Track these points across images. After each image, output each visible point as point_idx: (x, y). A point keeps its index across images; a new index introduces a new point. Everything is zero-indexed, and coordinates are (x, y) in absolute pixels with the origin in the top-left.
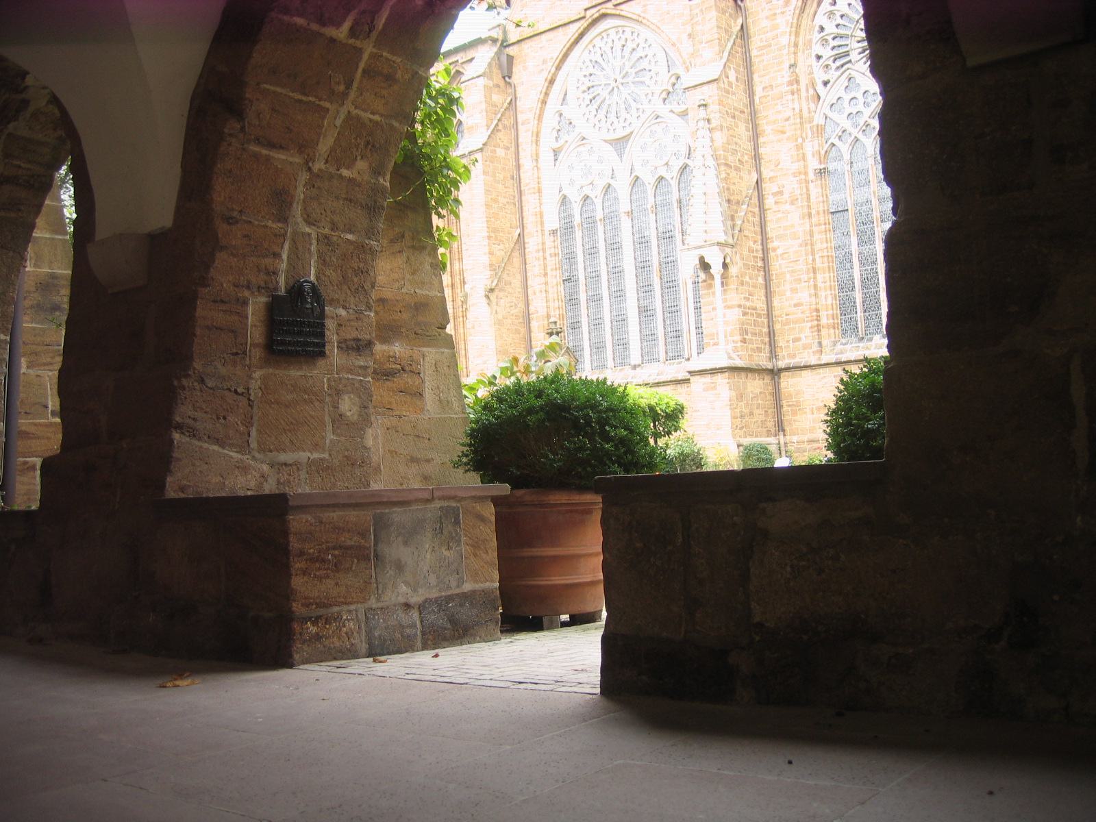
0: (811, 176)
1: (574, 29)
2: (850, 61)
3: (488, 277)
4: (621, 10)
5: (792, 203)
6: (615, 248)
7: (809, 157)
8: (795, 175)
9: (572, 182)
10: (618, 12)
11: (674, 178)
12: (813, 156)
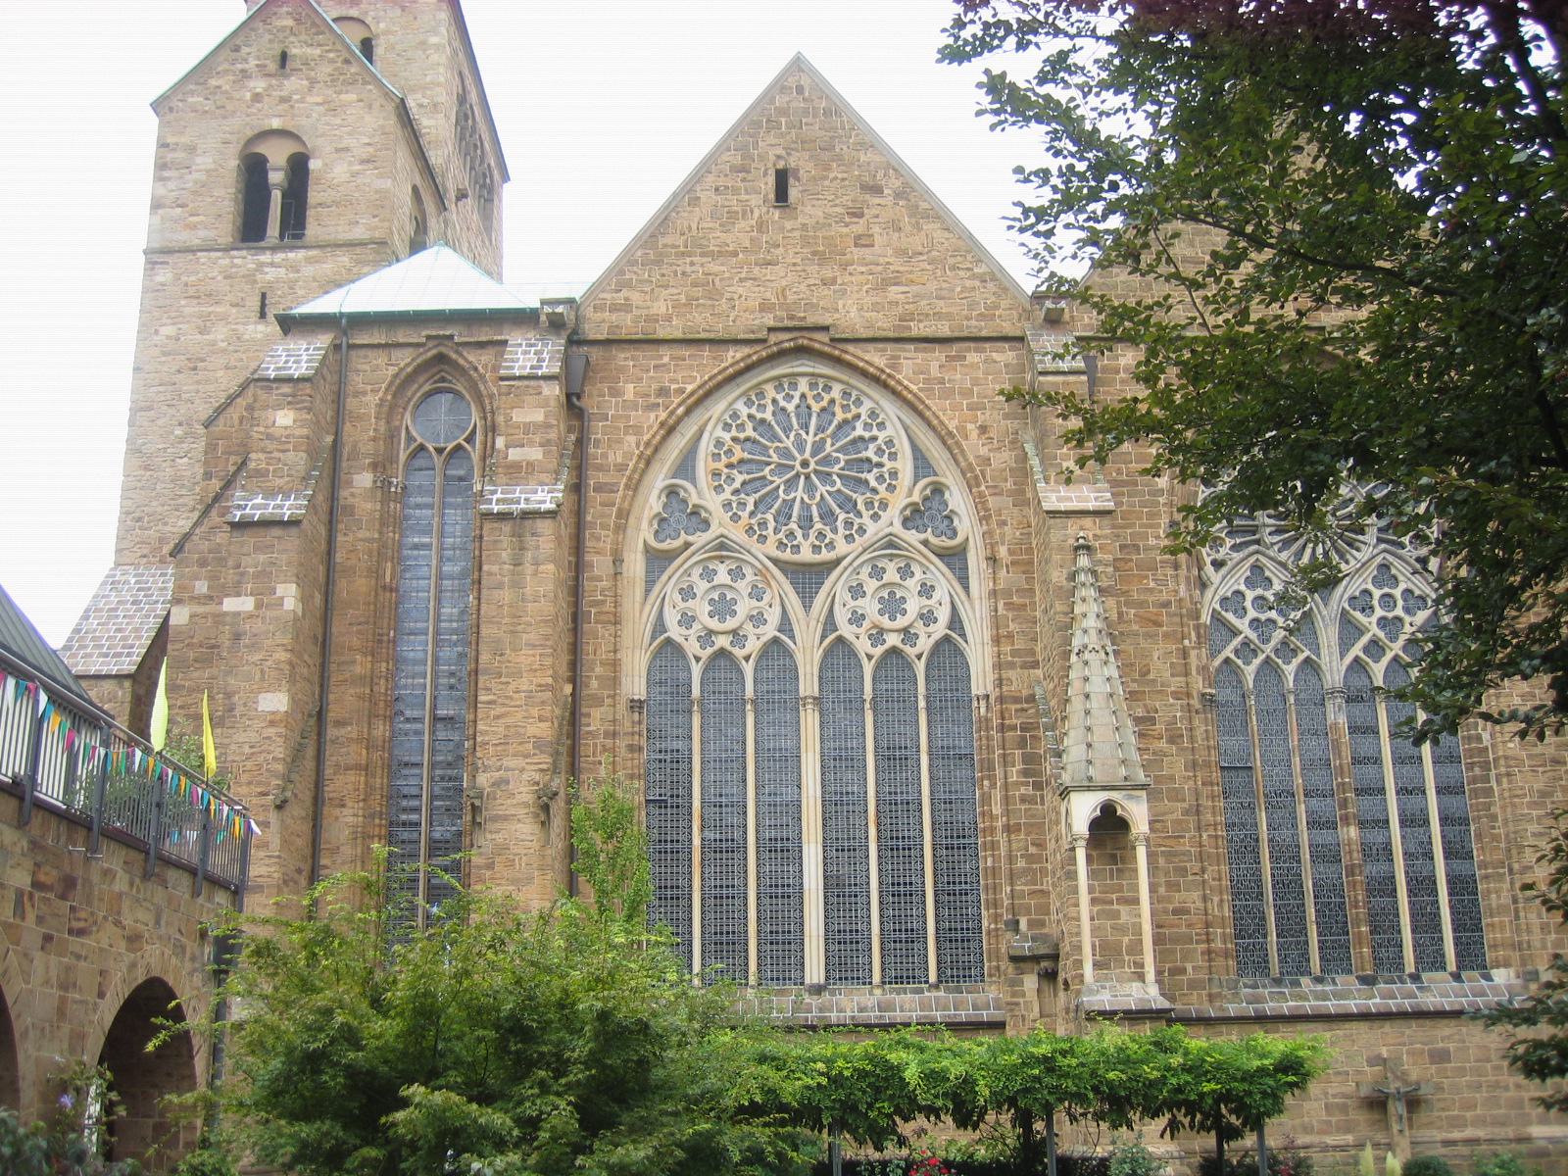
0: (1196, 703)
1: (734, 355)
2: (1257, 542)
3: (545, 766)
4: (846, 352)
5: (1172, 740)
6: (782, 762)
7: (1194, 673)
8: (1176, 695)
9: (687, 620)
10: (837, 352)
12: (1198, 673)
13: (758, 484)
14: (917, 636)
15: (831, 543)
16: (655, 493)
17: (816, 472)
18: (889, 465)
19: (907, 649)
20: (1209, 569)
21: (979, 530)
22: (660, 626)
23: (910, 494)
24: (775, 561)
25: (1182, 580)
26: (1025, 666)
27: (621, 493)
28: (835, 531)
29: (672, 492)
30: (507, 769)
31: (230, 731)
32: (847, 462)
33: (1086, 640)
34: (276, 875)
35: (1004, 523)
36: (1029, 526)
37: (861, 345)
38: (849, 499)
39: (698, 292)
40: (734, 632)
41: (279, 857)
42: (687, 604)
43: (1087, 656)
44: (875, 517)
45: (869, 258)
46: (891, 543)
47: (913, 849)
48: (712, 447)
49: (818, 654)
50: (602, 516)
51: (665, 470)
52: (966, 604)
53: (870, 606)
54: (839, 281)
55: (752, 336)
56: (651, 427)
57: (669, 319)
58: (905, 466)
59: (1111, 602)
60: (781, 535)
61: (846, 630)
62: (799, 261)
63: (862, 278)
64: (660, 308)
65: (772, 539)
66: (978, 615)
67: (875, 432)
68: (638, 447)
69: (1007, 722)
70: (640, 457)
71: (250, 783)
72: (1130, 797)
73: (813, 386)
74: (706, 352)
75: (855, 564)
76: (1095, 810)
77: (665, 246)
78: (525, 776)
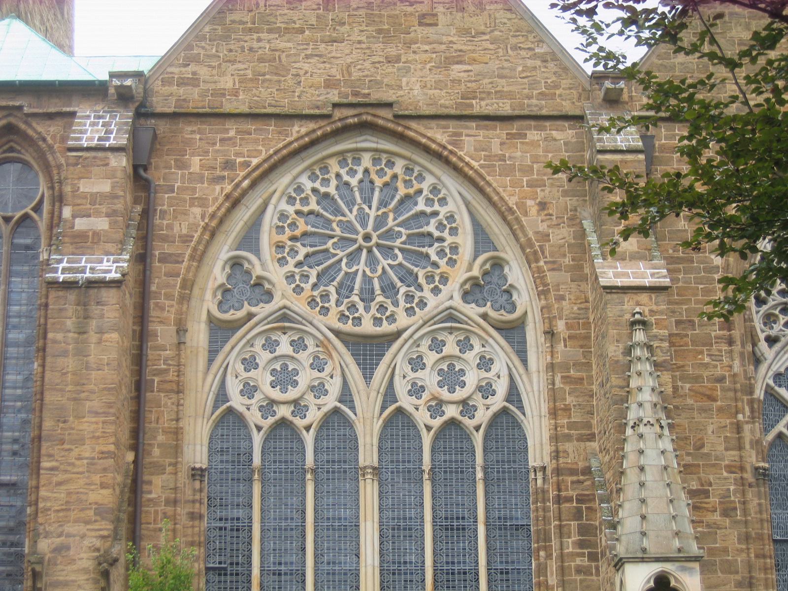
0: (749, 476)
1: (299, 130)
3: (105, 533)
4: (409, 128)
5: (725, 513)
7: (748, 446)
8: (730, 469)
9: (249, 390)
10: (400, 129)
11: (482, 431)
12: (752, 447)
13: (320, 257)
14: (475, 408)
15: (392, 315)
16: (219, 264)
17: (378, 245)
18: (449, 240)
19: (466, 421)
20: (763, 345)
21: (537, 304)
22: (222, 396)
23: (470, 268)
24: (337, 333)
25: (736, 356)
26: (580, 439)
27: (185, 264)
28: (396, 304)
29: (236, 263)
30: (69, 535)
32: (409, 236)
33: (641, 414)
35: (562, 298)
36: (587, 302)
37: (426, 122)
38: (410, 272)
39: (264, 67)
40: (295, 402)
42: (250, 374)
43: (642, 429)
44: (436, 291)
45: (434, 37)
46: (450, 316)
47: (414, 532)
48: (276, 221)
49: (378, 425)
50: (168, 286)
51: (230, 241)
52: (524, 377)
53: (429, 378)
54: (403, 60)
55: (317, 112)
56: (216, 199)
57: (235, 93)
58: (466, 241)
59: (666, 377)
60: (342, 308)
61: (406, 401)
62: (364, 39)
63: (425, 56)
64: (227, 82)
65: (334, 311)
66: (535, 388)
67: (436, 207)
68: (203, 217)
69: (563, 494)
70: (205, 228)
72: (684, 569)
73: (376, 161)
74: (272, 127)
75: (416, 336)
76: (648, 581)
77: (233, 22)
78: (86, 543)
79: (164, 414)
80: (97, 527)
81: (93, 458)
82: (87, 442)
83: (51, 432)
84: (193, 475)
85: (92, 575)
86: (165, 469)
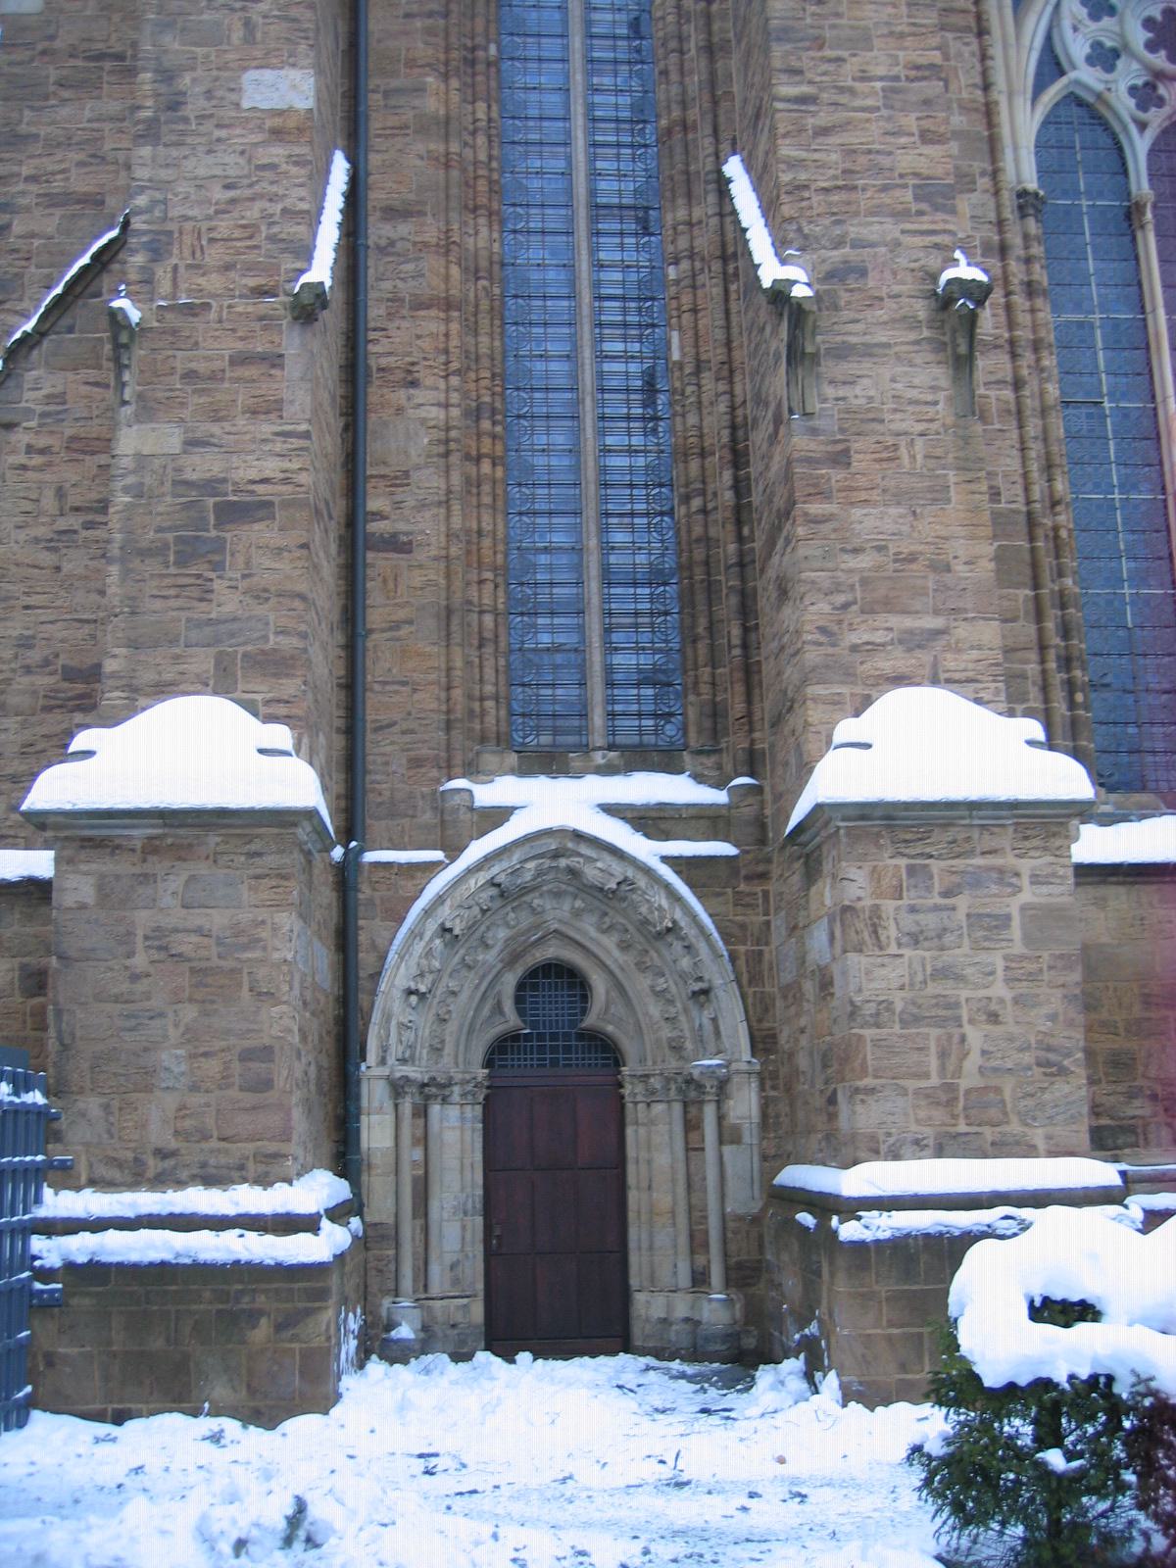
30: (859, 244)
31: (174, 152)
34: (304, 478)
41: (306, 435)
71: (228, 267)
79: (957, 76)
80: (925, 227)
81: (896, 78)
82: (876, 42)
83: (790, 23)
84: (1021, 207)
85: (926, 333)
86: (975, 183)
